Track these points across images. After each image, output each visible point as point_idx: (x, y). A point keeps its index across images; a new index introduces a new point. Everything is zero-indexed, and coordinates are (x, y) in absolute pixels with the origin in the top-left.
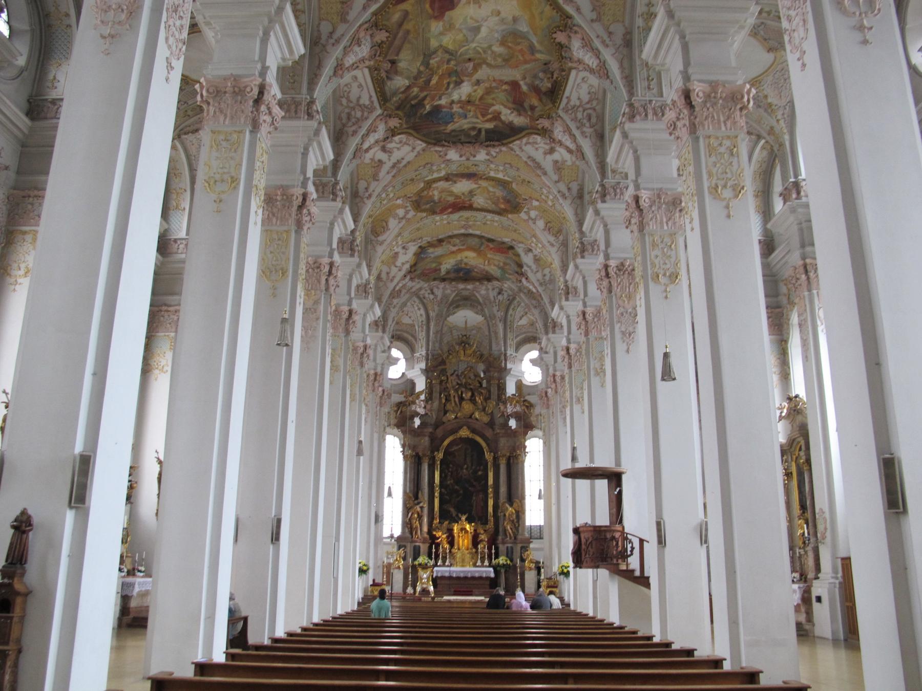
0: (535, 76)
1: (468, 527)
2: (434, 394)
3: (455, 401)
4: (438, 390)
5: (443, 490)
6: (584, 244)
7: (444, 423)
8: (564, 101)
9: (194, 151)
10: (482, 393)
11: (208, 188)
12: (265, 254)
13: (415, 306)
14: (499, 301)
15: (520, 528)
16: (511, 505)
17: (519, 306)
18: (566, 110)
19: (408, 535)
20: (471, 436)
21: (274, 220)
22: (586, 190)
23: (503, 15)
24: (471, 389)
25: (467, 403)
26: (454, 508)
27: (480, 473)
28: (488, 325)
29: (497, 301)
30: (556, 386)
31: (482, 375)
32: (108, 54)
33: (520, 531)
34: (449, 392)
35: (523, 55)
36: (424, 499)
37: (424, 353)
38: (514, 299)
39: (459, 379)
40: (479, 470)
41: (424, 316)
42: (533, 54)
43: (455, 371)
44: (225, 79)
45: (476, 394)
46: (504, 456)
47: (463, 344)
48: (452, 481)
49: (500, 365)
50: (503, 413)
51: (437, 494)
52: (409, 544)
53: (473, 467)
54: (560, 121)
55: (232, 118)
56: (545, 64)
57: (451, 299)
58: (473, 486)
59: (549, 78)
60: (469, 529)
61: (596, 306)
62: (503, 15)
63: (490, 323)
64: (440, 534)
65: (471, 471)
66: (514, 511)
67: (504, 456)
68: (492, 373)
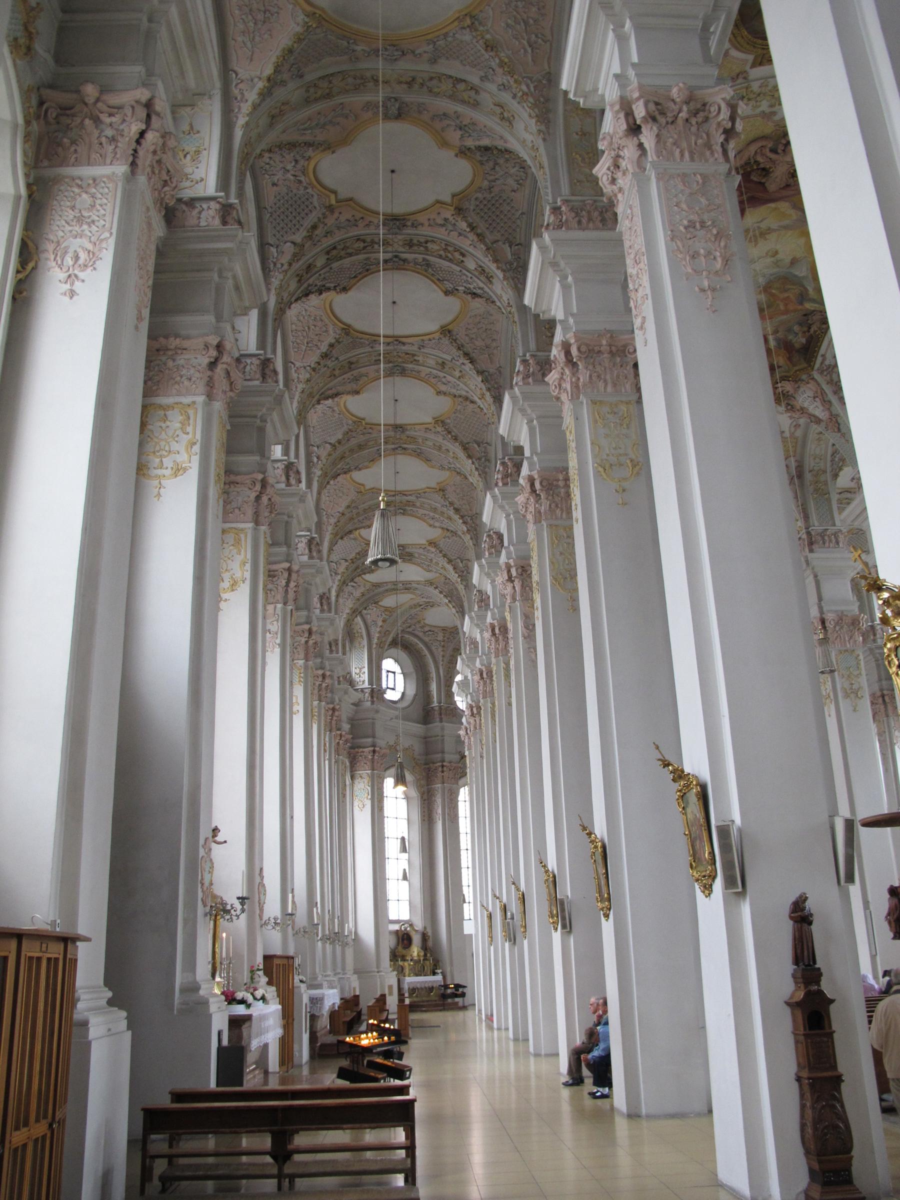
0: (789, 330)
6: (811, 535)
8: (819, 359)
9: (314, 421)
11: (603, 473)
12: (553, 555)
18: (821, 372)
21: (558, 512)
22: (806, 468)
23: (779, 256)
32: (715, 311)
35: (786, 305)
42: (801, 304)
44: (600, 336)
54: (812, 385)
55: (615, 385)
56: (805, 315)
59: (804, 332)
61: (836, 611)
62: (779, 256)
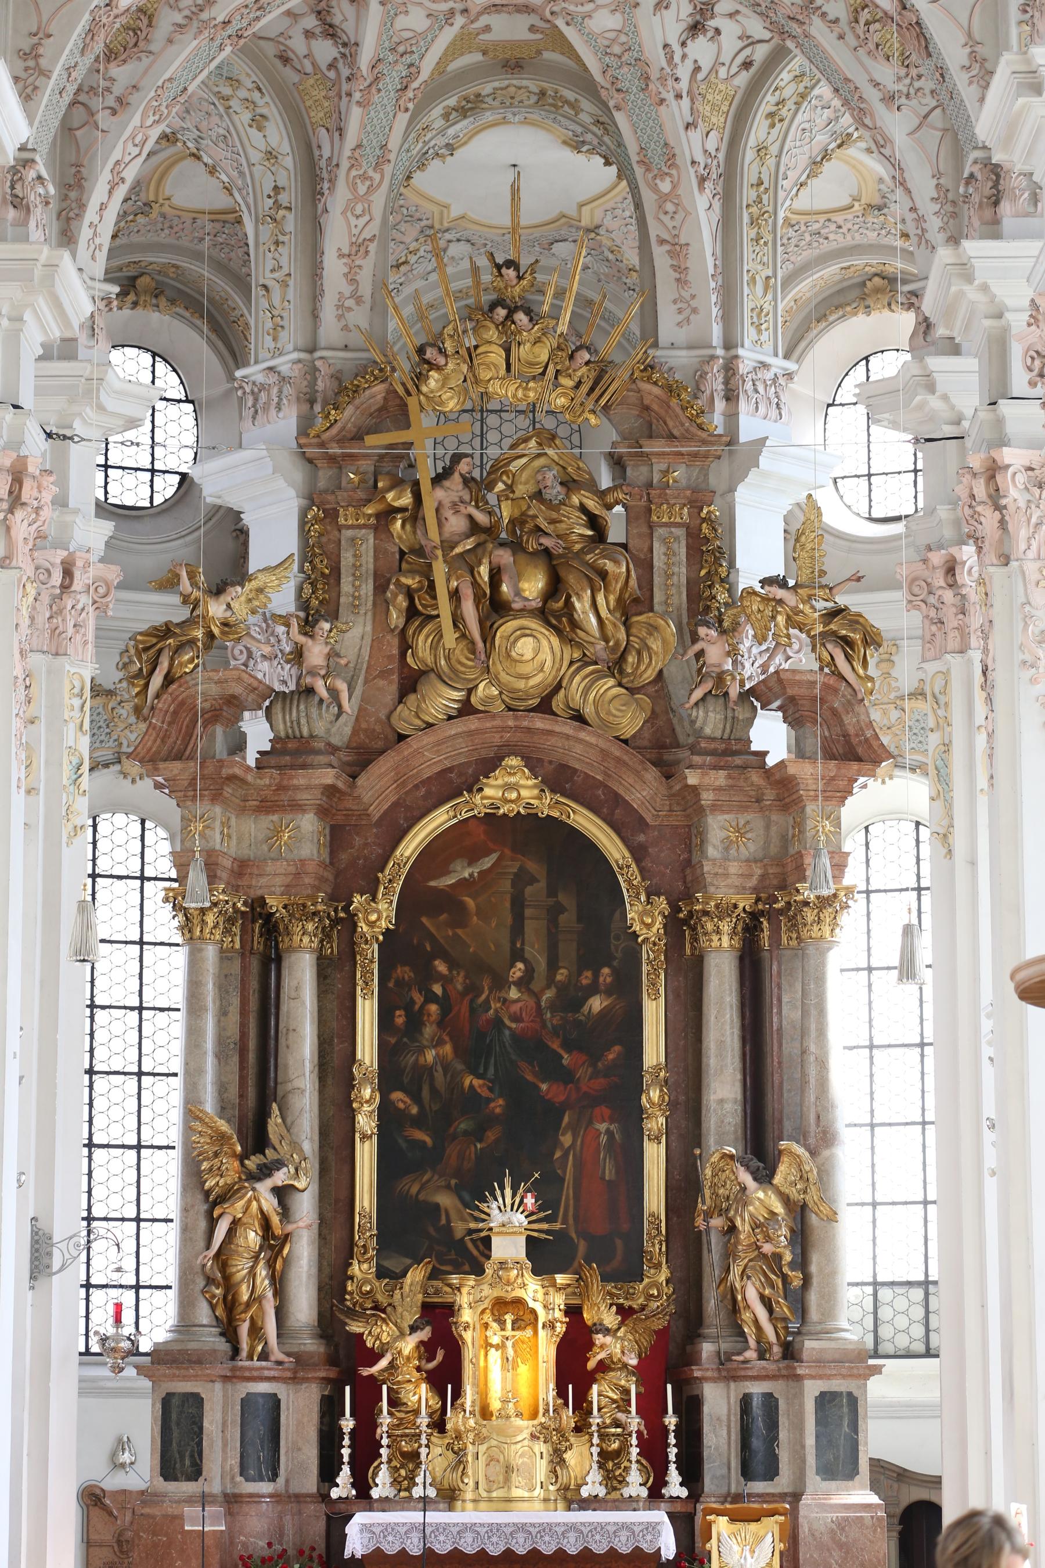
2: (346, 586)
3: (457, 620)
4: (368, 561)
5: (398, 1096)
7: (401, 738)
10: (603, 575)
13: (234, 103)
14: (697, 69)
15: (813, 1298)
16: (765, 1175)
17: (803, 96)
19: (212, 1340)
20: (546, 805)
24: (547, 553)
25: (525, 632)
26: (457, 1191)
27: (596, 1004)
28: (638, 205)
29: (684, 72)
30: (1003, 523)
31: (605, 481)
33: (814, 1314)
34: (427, 573)
36: (296, 1146)
37: (285, 363)
38: (778, 57)
39: (479, 501)
40: (593, 989)
41: (288, 162)
43: (457, 458)
45: (571, 579)
47: (501, 313)
48: (448, 1049)
49: (698, 421)
50: (720, 679)
51: (366, 1121)
52: (218, 1386)
53: (561, 975)
57: (427, 67)
58: (566, 1076)
60: (538, 1307)
63: (648, 198)
64: (386, 1332)
65: (549, 994)
66: (779, 1208)
67: (726, 910)
68: (659, 466)
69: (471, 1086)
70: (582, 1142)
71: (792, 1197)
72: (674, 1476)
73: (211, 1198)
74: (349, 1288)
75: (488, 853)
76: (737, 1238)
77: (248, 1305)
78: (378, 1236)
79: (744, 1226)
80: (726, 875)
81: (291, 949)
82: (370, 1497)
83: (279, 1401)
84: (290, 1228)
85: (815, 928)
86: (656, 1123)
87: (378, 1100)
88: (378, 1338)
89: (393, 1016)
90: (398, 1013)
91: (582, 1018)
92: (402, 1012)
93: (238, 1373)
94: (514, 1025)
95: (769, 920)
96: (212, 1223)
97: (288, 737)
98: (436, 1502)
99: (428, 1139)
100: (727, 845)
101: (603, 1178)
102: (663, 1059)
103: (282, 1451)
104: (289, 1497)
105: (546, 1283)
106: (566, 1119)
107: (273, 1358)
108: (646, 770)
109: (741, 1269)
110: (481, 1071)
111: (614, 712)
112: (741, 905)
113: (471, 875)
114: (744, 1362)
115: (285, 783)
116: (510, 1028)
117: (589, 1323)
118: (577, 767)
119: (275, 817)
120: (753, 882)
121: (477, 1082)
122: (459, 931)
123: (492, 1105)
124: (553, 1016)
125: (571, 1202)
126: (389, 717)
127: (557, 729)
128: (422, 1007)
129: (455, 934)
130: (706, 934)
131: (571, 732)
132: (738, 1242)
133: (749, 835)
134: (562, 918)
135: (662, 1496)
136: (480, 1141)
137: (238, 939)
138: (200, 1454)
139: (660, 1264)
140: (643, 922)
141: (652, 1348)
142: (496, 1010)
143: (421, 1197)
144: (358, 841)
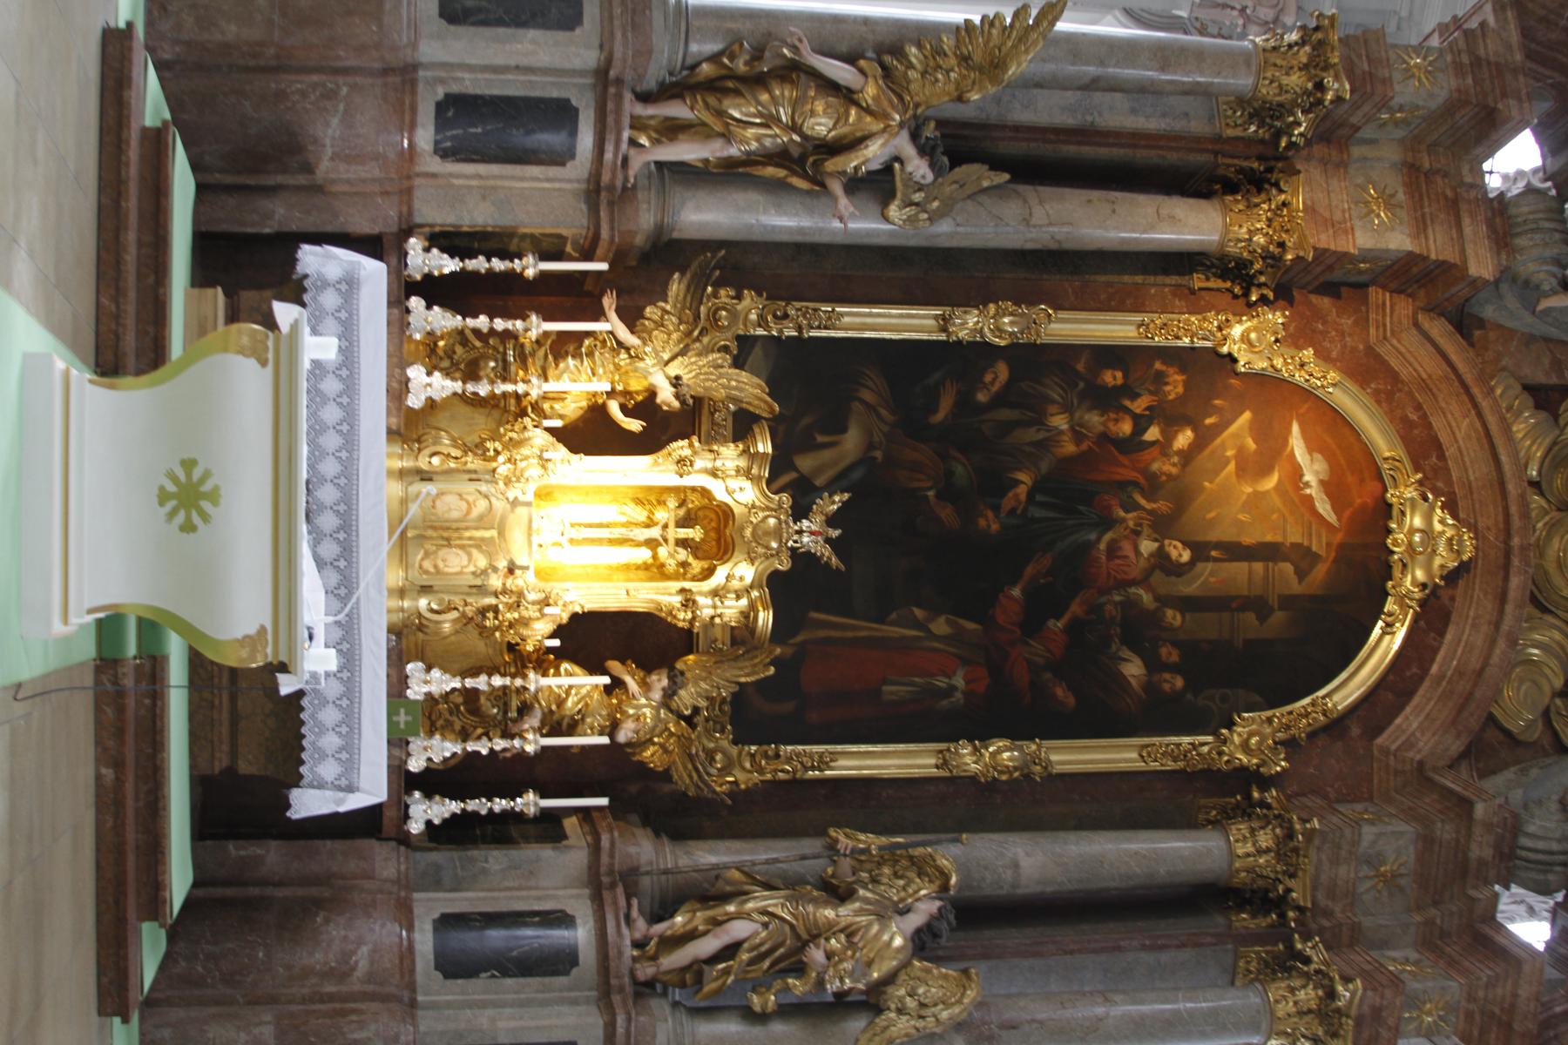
1: (742, 571)
5: (1002, 372)
16: (924, 943)
26: (865, 460)
27: (1133, 669)
40: (1154, 665)
46: (1286, 849)
48: (1069, 448)
51: (969, 324)
53: (1173, 617)
58: (1032, 624)
60: (718, 578)
65: (1146, 598)
69: (1018, 482)
70: (935, 650)
71: (890, 989)
72: (443, 809)
73: (887, 59)
74: (722, 292)
75: (1337, 507)
76: (826, 904)
77: (721, 114)
78: (799, 339)
79: (845, 913)
80: (1335, 861)
81: (1226, 210)
82: (408, 297)
83: (563, 164)
84: (836, 187)
85: (1291, 1008)
86: (968, 759)
87: (1003, 343)
88: (660, 324)
89: (1114, 368)
90: (1119, 375)
91: (1114, 647)
92: (1120, 381)
93: (612, 90)
94: (1102, 546)
95: (1272, 926)
96: (851, 59)
97: (1509, 217)
98: (399, 409)
99: (940, 416)
100: (1374, 861)
101: (885, 682)
102: (1058, 769)
103: (482, 168)
104: (409, 177)
105: (755, 594)
106: (970, 625)
107: (632, 152)
108: (1458, 736)
109: (778, 911)
110: (1039, 498)
111: (1524, 688)
112: (1291, 883)
113: (1307, 485)
114: (628, 918)
115: (1463, 207)
116: (1099, 540)
117: (679, 665)
118: (1449, 637)
119: (1401, 196)
120: (1323, 901)
121: (1022, 491)
122: (1232, 467)
123: (990, 514)
124: (1116, 604)
125: (849, 634)
126: (1503, 369)
127: (1509, 608)
128: (1127, 411)
129: (1227, 462)
130: (1253, 831)
131: (1505, 627)
132: (814, 901)
133: (1385, 893)
134: (1250, 617)
135: (409, 791)
136: (938, 496)
137: (1238, 132)
138: (485, 23)
139: (761, 771)
140: (1251, 735)
141: (642, 765)
142: (1124, 520)
143: (856, 406)
144: (1347, 322)
